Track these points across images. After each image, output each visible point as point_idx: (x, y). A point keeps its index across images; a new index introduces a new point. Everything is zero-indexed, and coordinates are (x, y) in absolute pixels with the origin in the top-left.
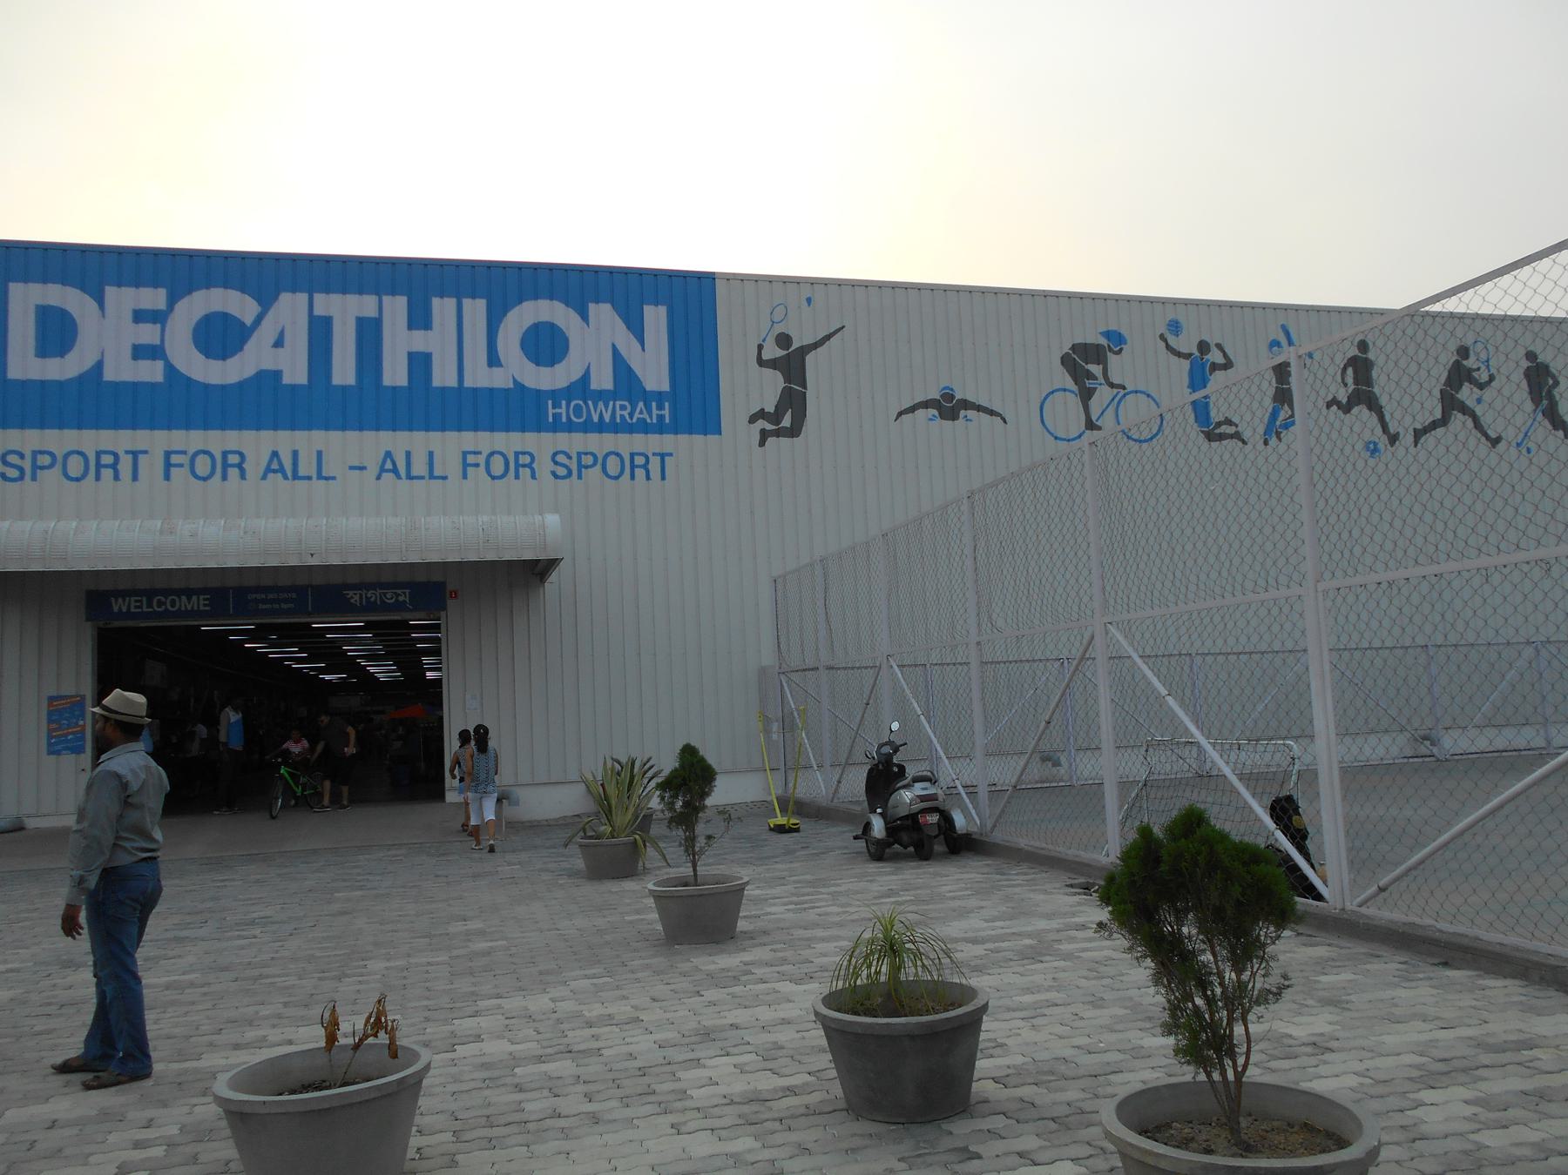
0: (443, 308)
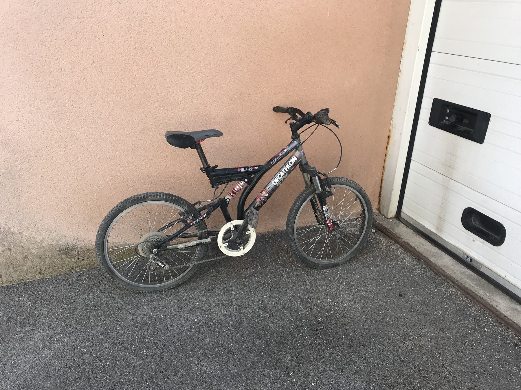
0: (286, 166)
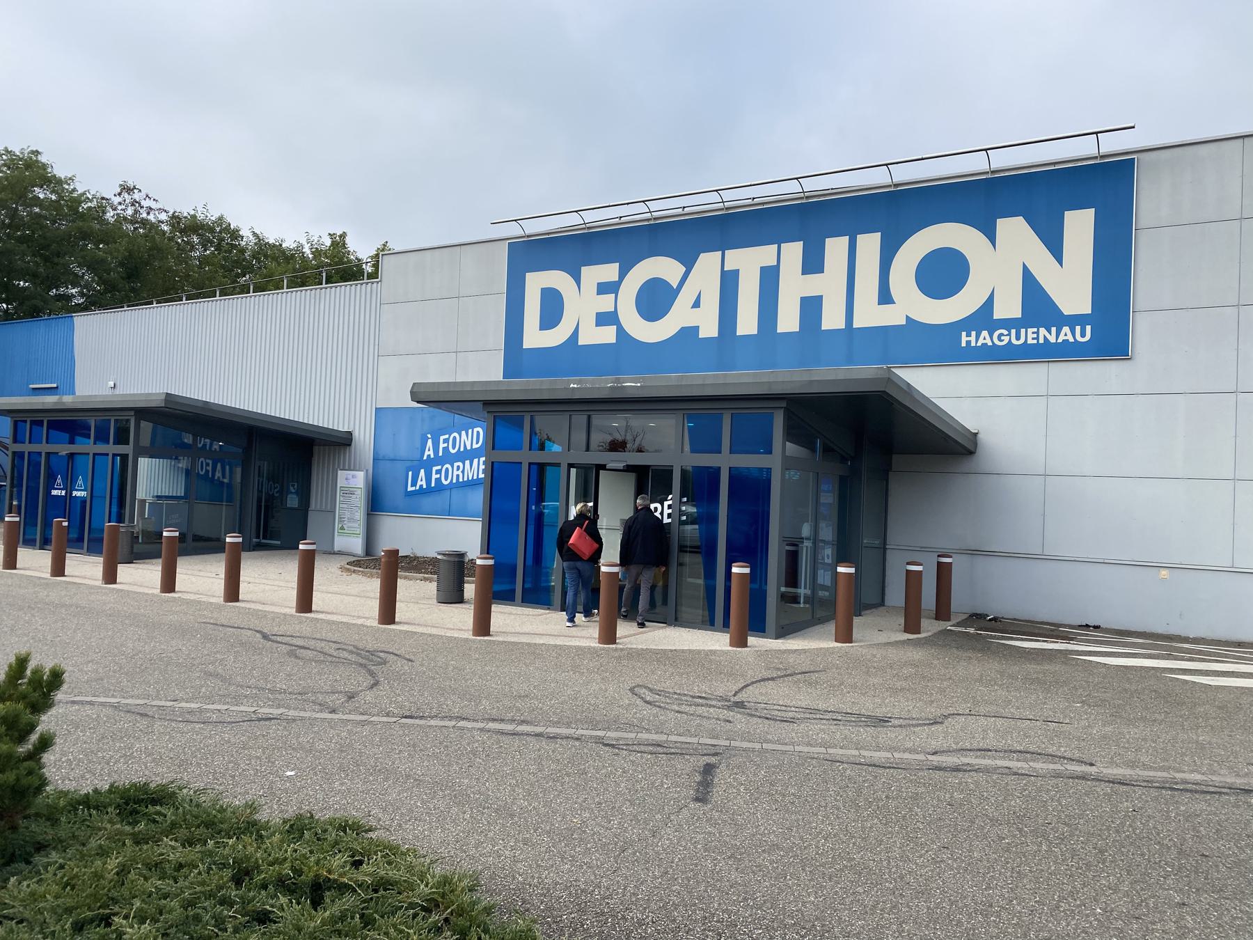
0: (836, 248)
